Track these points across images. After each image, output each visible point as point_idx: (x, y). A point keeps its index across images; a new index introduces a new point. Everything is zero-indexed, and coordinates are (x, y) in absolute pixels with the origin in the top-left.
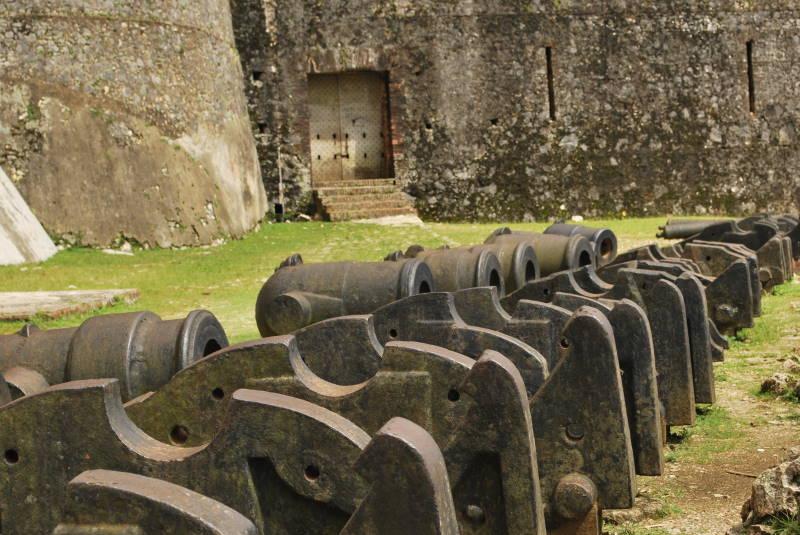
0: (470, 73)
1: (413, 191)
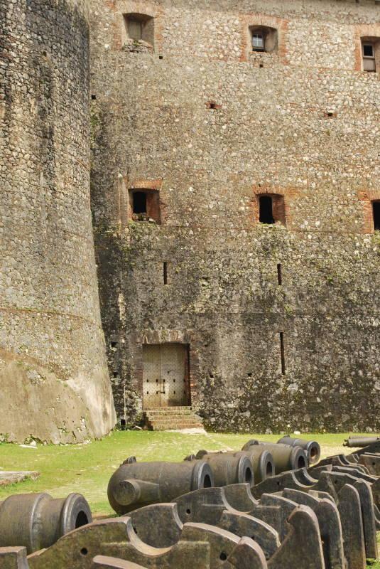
0: (236, 346)
1: (202, 414)
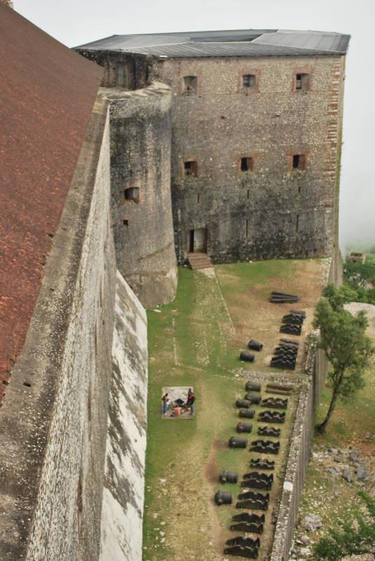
1: (211, 257)
